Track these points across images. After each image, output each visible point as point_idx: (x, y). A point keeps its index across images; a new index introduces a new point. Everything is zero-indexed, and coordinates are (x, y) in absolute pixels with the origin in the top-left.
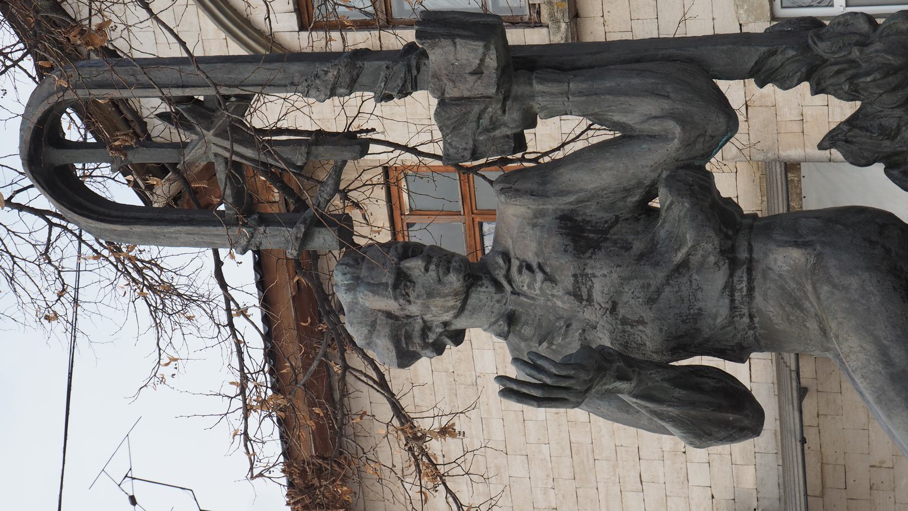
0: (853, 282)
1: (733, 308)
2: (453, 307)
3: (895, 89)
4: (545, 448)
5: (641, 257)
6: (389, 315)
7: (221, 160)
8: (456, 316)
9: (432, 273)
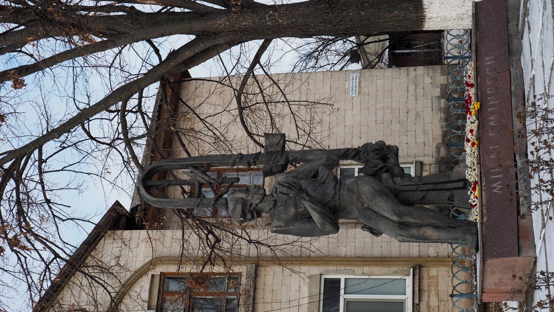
1: (335, 192)
2: (260, 198)
3: (377, 154)
6: (242, 198)
7: (198, 182)
8: (260, 202)
9: (256, 189)
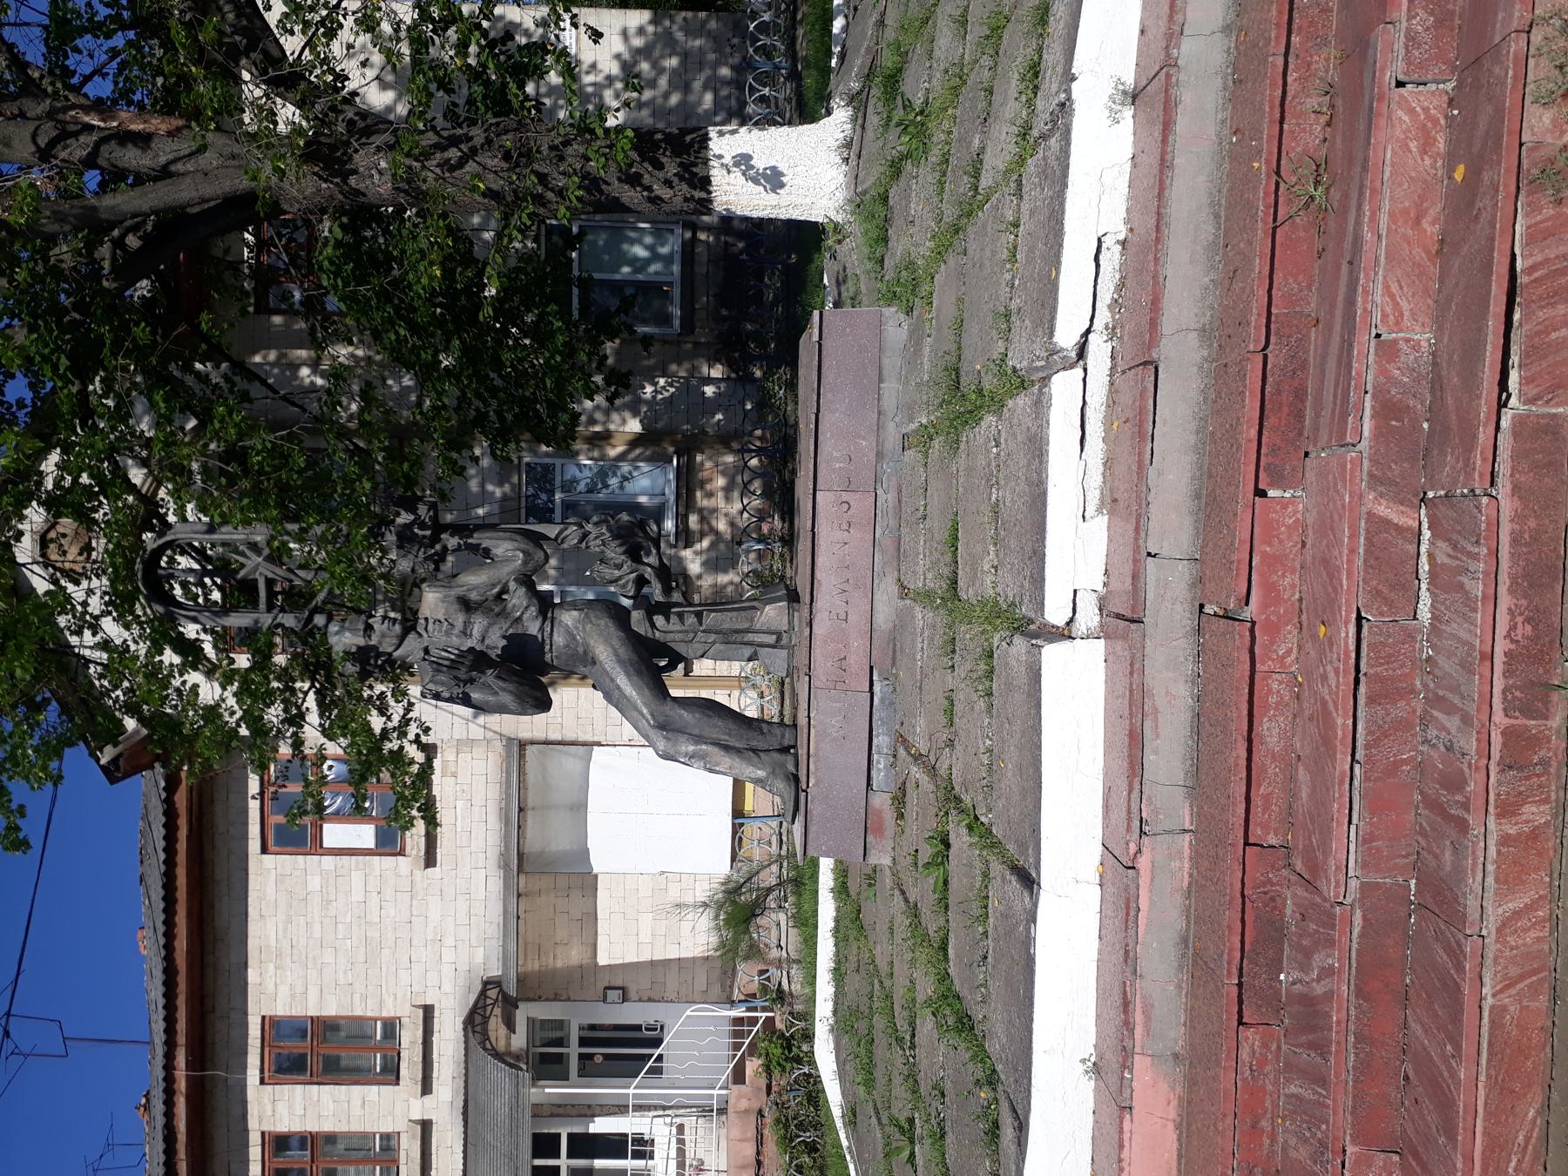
0: (602, 622)
4: (348, 941)
5: (498, 615)
